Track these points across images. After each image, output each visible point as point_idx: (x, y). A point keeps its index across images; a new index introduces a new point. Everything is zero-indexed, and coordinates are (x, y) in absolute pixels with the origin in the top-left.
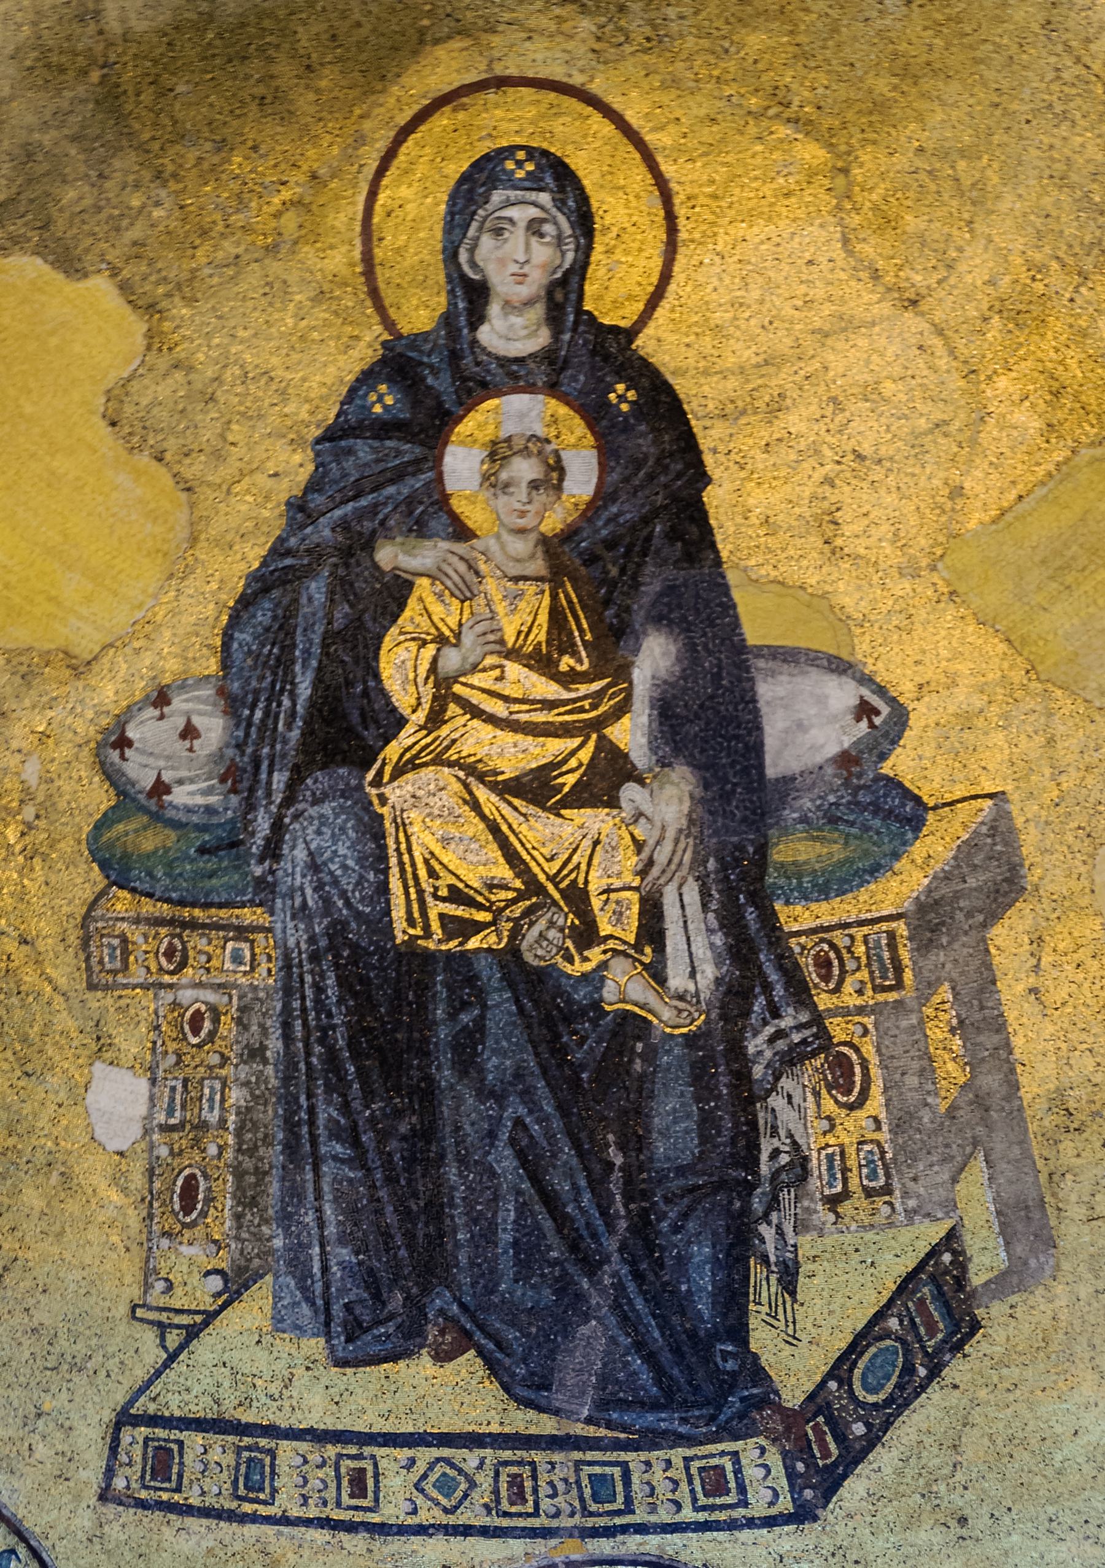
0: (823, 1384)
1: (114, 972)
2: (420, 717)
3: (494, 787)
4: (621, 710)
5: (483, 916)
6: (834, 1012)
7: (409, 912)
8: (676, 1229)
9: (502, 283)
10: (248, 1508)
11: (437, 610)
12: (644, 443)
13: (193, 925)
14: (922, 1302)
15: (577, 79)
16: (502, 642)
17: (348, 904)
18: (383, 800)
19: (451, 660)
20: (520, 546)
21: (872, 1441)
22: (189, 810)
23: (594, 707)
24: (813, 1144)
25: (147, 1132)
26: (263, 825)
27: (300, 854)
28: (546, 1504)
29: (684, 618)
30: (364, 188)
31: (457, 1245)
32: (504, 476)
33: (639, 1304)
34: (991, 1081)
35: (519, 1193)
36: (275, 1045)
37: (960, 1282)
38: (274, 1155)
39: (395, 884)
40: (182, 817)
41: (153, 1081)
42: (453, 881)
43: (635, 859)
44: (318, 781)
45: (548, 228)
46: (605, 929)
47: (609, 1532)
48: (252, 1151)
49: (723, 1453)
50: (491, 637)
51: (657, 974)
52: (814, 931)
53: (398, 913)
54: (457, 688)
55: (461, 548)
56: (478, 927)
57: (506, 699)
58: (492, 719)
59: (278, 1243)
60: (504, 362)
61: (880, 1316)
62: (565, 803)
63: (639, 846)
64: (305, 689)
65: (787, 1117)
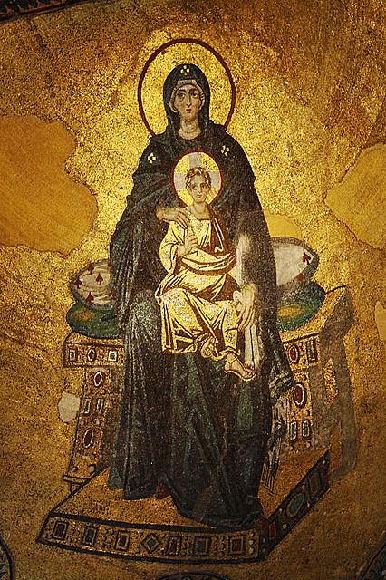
0: (278, 509)
1: (73, 361)
2: (170, 272)
3: (194, 294)
4: (234, 263)
5: (190, 341)
6: (297, 371)
7: (167, 340)
8: (242, 453)
9: (184, 114)
10: (84, 547)
11: (177, 233)
12: (233, 167)
13: (99, 345)
14: (313, 478)
15: (198, 37)
16: (197, 243)
17: (148, 338)
18: (160, 301)
19: (182, 250)
20: (200, 208)
21: (289, 530)
22: (99, 305)
23: (225, 264)
24: (287, 421)
25: (78, 416)
26: (123, 311)
27: (134, 320)
28: (183, 553)
29: (251, 230)
30: (137, 83)
31: (171, 458)
32: (193, 183)
33: (226, 480)
34: (344, 395)
35: (193, 439)
36: (122, 387)
37: (326, 471)
38: (117, 425)
39: (163, 330)
40: (97, 308)
41: (81, 399)
42: (180, 328)
43: (236, 318)
44: (141, 294)
45: (196, 92)
46: (227, 344)
47: (199, 562)
48: (110, 424)
49: (242, 535)
50: (193, 242)
51: (242, 360)
52: (291, 341)
53: (164, 340)
54: (183, 260)
55: (183, 210)
56: (188, 344)
57: (198, 263)
58: (194, 271)
59: (114, 456)
60: (187, 141)
61: (300, 484)
62: (217, 299)
63: (238, 313)
64: (136, 263)
65: (281, 411)
